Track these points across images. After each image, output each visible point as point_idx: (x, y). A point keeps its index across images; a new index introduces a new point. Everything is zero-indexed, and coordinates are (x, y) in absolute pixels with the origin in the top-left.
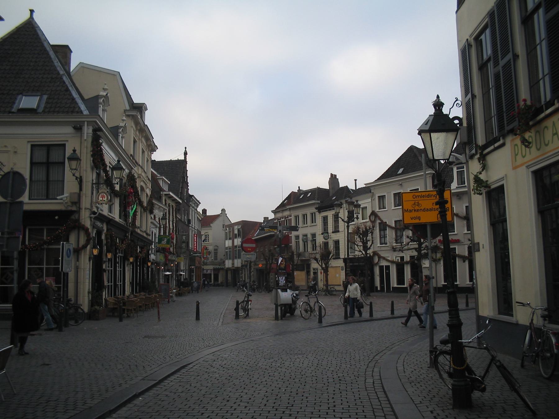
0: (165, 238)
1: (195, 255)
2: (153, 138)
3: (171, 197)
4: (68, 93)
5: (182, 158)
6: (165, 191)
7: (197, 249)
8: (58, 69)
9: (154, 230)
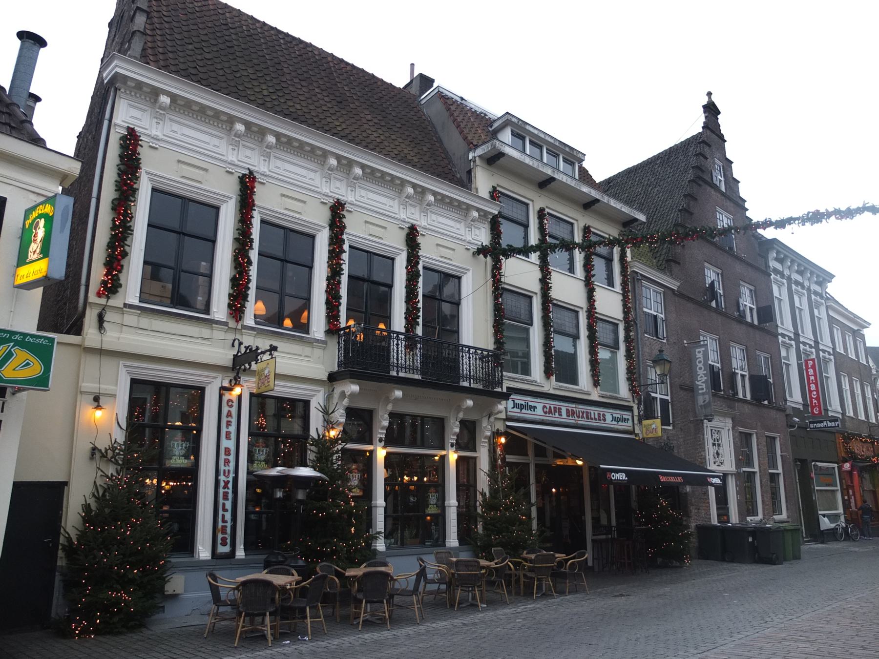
1: (819, 425)
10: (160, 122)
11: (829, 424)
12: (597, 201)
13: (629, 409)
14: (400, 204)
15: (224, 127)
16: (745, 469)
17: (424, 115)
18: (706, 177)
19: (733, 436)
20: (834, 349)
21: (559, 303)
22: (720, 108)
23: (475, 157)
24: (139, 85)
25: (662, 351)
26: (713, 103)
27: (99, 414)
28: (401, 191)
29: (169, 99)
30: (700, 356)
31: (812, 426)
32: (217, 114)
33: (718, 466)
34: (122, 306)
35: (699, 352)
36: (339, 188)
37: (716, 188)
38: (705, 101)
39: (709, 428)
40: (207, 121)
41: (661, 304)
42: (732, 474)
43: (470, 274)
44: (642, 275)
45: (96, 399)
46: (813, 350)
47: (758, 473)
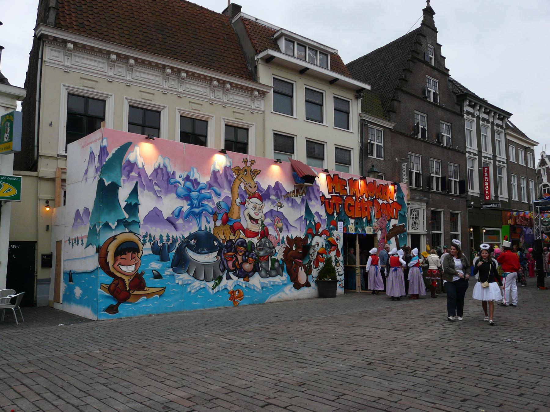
1: (488, 206)
7: (489, 195)
10: (69, 57)
11: (494, 206)
12: (337, 79)
14: (210, 90)
15: (105, 57)
16: (433, 232)
17: (233, 30)
18: (420, 57)
19: (426, 213)
20: (508, 159)
21: (311, 140)
22: (435, 11)
23: (258, 59)
24: (55, 39)
25: (374, 166)
26: (430, 7)
27: (48, 209)
28: (211, 83)
29: (72, 45)
30: (404, 167)
31: (484, 206)
32: (100, 51)
33: (414, 230)
34: (57, 156)
35: (404, 165)
36: (173, 85)
37: (428, 64)
38: (425, 6)
39: (410, 209)
40: (95, 54)
41: (382, 137)
42: (424, 235)
43: (254, 127)
44: (367, 121)
45: (47, 202)
46: (492, 161)
47: (443, 234)
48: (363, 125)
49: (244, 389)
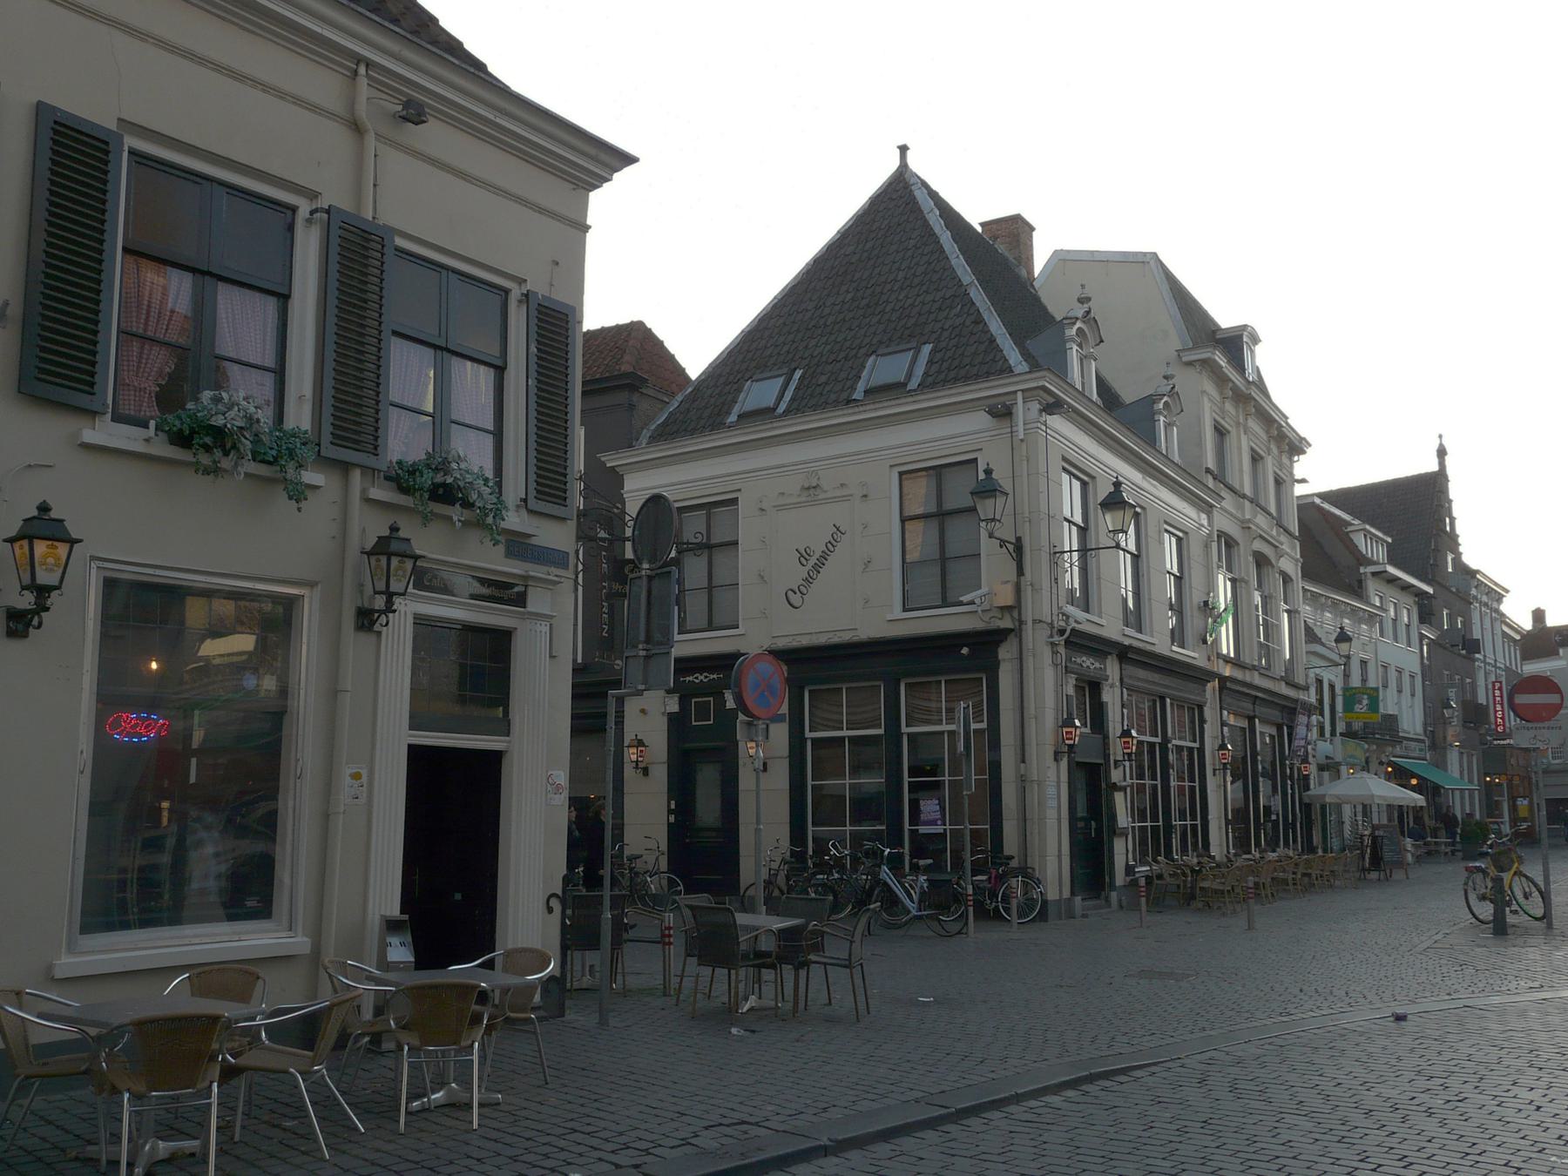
0: (1363, 694)
1: (1502, 742)
2: (1287, 418)
3: (1393, 580)
4: (981, 325)
5: (1432, 466)
6: (1371, 562)
8: (959, 272)
9: (1327, 676)
13: (1423, 741)
31: (1495, 742)
48: (1422, 637)
49: (582, 1166)
